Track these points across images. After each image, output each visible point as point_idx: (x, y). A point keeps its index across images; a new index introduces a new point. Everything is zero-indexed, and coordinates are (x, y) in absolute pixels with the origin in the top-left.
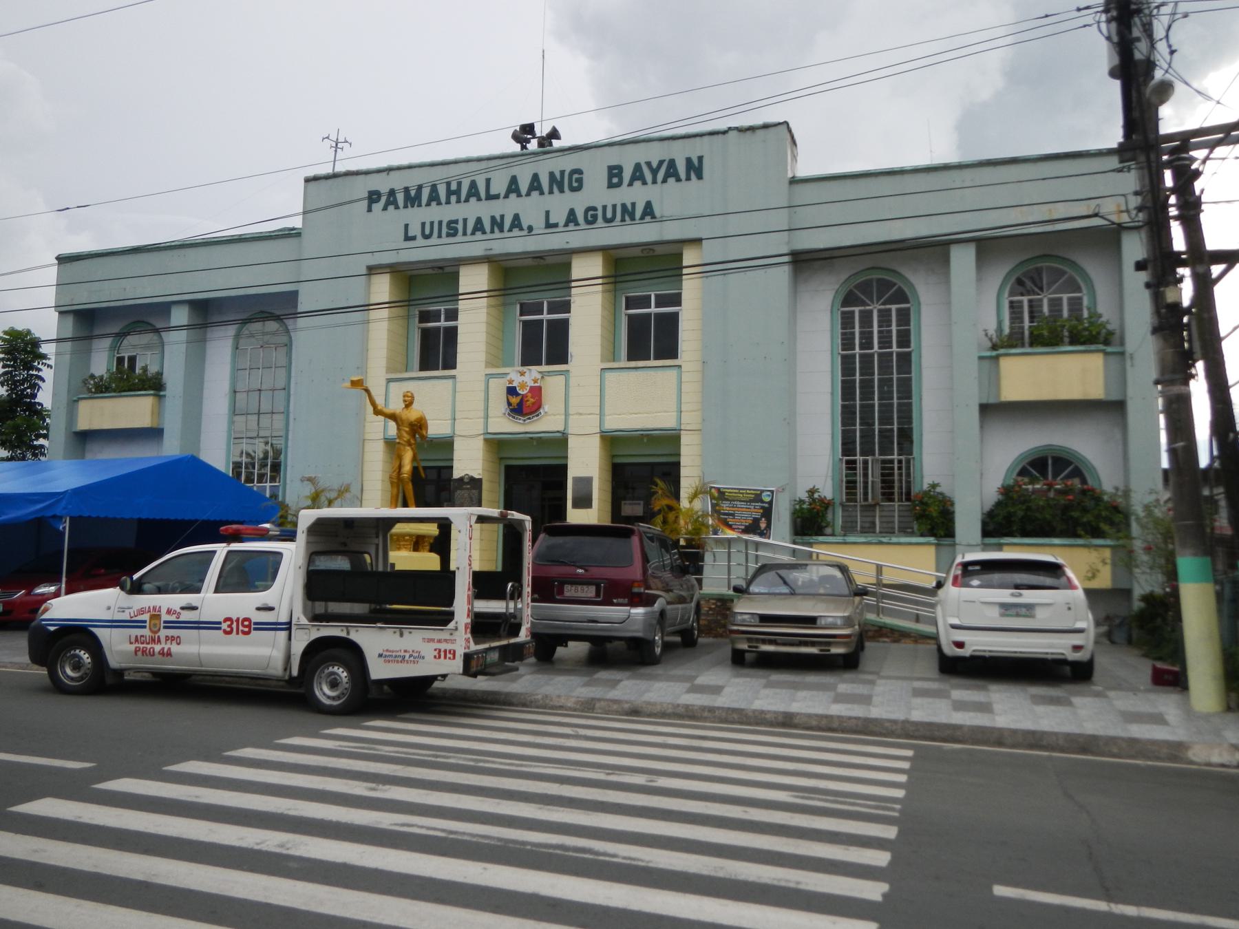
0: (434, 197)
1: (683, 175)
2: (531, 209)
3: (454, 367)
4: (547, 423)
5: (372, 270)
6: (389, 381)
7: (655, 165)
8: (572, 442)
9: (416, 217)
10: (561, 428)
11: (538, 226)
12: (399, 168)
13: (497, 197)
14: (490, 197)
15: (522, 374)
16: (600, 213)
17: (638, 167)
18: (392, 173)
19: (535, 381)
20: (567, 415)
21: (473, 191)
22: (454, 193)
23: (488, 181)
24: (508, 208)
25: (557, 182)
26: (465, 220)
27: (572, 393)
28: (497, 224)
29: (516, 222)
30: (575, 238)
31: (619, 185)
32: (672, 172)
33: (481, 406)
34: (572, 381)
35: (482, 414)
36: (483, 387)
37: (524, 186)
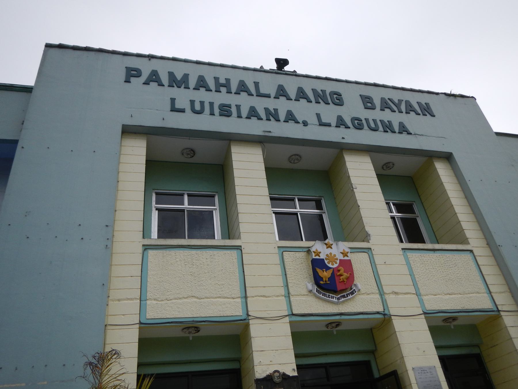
0: (202, 84)
1: (420, 112)
2: (304, 110)
3: (239, 238)
4: (363, 302)
5: (128, 131)
6: (146, 248)
7: (397, 102)
8: (398, 324)
9: (183, 97)
10: (381, 309)
11: (310, 125)
12: (162, 58)
13: (268, 96)
14: (260, 95)
15: (329, 246)
16: (364, 122)
17: (383, 100)
18: (153, 60)
19: (345, 254)
20: (382, 294)
21: (242, 88)
22: (223, 85)
23: (256, 84)
24: (282, 106)
25: (320, 97)
26: (238, 107)
27: (381, 269)
28: (272, 115)
29: (290, 117)
30: (352, 136)
31: (373, 108)
32: (410, 109)
33: (280, 281)
34: (378, 260)
35: (282, 291)
36: (277, 259)
37: (293, 94)
